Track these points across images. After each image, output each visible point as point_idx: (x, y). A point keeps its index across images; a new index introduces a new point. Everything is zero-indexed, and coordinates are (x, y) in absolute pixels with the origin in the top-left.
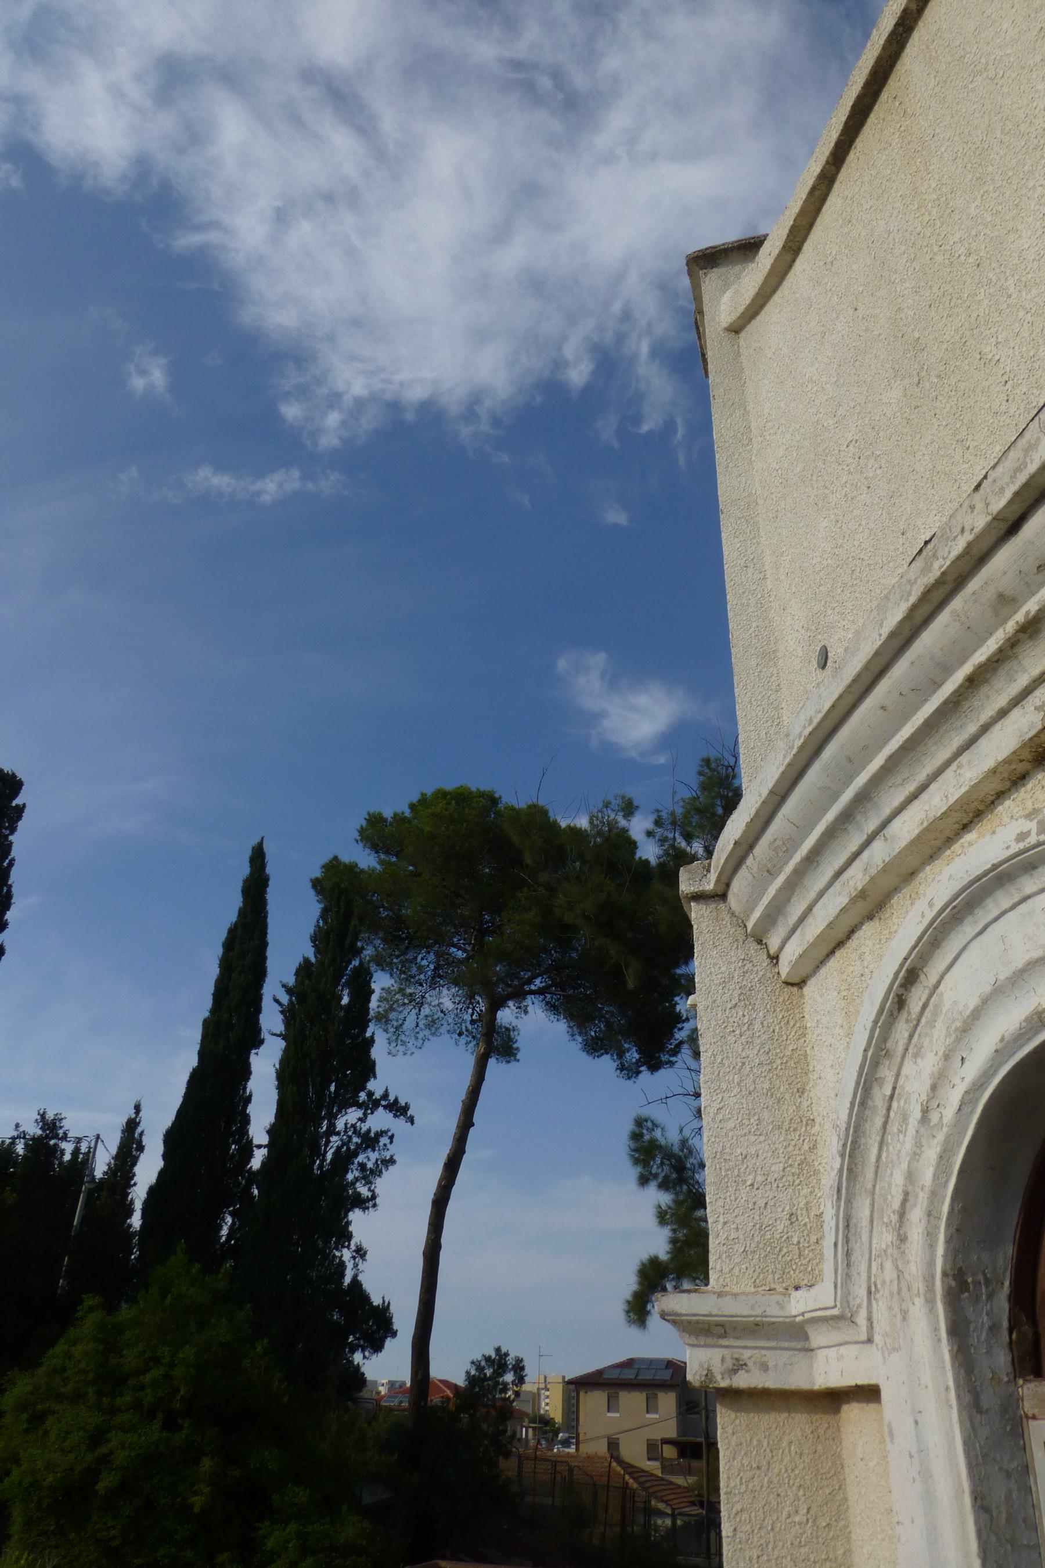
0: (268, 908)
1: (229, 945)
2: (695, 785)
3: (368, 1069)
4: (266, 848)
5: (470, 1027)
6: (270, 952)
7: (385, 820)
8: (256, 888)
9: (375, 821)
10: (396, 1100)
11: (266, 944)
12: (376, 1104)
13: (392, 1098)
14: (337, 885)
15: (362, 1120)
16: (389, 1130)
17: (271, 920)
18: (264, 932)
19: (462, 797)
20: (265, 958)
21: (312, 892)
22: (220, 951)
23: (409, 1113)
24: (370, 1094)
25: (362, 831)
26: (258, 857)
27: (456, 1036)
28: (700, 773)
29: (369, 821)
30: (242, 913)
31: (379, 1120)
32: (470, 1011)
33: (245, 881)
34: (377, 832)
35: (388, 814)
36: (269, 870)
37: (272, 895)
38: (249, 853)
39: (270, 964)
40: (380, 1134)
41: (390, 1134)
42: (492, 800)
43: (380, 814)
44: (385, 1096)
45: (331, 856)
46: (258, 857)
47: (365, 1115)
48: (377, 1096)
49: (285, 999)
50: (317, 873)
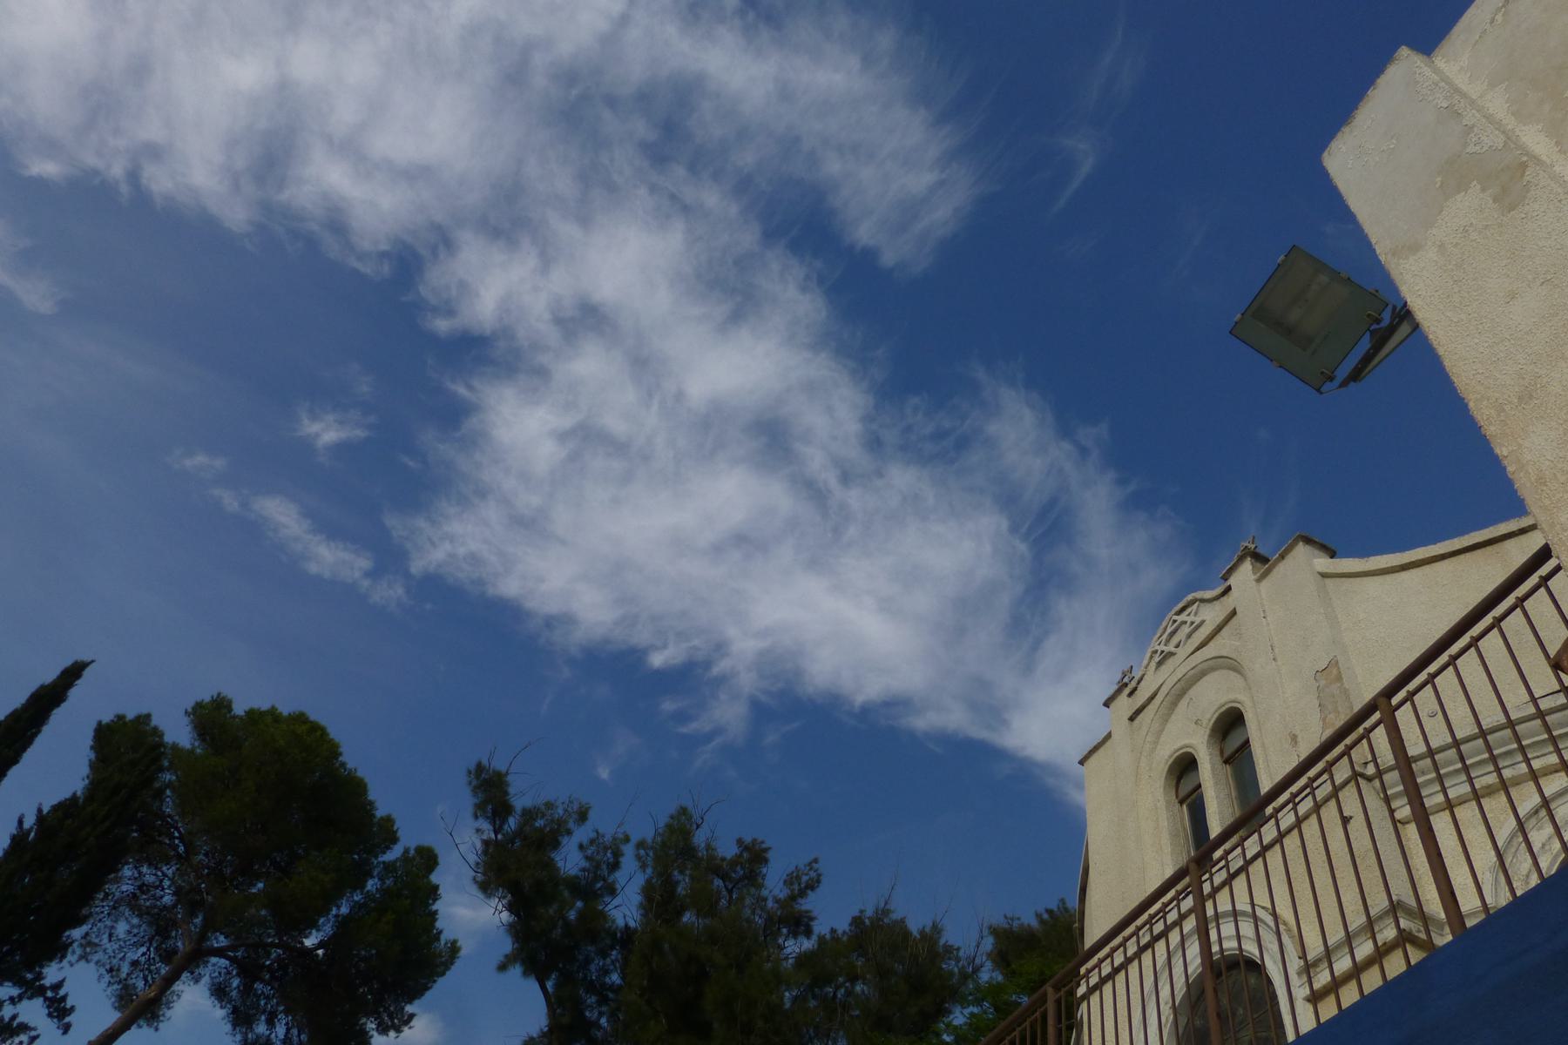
0: (45, 729)
2: (661, 825)
3: (57, 950)
5: (125, 969)
7: (230, 710)
9: (221, 705)
10: (64, 998)
11: (14, 760)
12: (40, 991)
13: (62, 992)
14: (125, 746)
15: (12, 1000)
16: (34, 1029)
17: (39, 741)
18: (24, 749)
19: (317, 730)
23: (67, 1020)
24: (39, 976)
25: (199, 706)
27: (103, 971)
28: (672, 817)
29: (213, 701)
30: (15, 716)
31: (33, 1012)
32: (144, 949)
33: (42, 687)
34: (211, 718)
35: (239, 709)
37: (58, 716)
40: (24, 1028)
41: (33, 1033)
42: (334, 751)
44: (57, 986)
45: (145, 712)
47: (20, 997)
48: (47, 982)
49: (29, 822)
50: (155, 722)
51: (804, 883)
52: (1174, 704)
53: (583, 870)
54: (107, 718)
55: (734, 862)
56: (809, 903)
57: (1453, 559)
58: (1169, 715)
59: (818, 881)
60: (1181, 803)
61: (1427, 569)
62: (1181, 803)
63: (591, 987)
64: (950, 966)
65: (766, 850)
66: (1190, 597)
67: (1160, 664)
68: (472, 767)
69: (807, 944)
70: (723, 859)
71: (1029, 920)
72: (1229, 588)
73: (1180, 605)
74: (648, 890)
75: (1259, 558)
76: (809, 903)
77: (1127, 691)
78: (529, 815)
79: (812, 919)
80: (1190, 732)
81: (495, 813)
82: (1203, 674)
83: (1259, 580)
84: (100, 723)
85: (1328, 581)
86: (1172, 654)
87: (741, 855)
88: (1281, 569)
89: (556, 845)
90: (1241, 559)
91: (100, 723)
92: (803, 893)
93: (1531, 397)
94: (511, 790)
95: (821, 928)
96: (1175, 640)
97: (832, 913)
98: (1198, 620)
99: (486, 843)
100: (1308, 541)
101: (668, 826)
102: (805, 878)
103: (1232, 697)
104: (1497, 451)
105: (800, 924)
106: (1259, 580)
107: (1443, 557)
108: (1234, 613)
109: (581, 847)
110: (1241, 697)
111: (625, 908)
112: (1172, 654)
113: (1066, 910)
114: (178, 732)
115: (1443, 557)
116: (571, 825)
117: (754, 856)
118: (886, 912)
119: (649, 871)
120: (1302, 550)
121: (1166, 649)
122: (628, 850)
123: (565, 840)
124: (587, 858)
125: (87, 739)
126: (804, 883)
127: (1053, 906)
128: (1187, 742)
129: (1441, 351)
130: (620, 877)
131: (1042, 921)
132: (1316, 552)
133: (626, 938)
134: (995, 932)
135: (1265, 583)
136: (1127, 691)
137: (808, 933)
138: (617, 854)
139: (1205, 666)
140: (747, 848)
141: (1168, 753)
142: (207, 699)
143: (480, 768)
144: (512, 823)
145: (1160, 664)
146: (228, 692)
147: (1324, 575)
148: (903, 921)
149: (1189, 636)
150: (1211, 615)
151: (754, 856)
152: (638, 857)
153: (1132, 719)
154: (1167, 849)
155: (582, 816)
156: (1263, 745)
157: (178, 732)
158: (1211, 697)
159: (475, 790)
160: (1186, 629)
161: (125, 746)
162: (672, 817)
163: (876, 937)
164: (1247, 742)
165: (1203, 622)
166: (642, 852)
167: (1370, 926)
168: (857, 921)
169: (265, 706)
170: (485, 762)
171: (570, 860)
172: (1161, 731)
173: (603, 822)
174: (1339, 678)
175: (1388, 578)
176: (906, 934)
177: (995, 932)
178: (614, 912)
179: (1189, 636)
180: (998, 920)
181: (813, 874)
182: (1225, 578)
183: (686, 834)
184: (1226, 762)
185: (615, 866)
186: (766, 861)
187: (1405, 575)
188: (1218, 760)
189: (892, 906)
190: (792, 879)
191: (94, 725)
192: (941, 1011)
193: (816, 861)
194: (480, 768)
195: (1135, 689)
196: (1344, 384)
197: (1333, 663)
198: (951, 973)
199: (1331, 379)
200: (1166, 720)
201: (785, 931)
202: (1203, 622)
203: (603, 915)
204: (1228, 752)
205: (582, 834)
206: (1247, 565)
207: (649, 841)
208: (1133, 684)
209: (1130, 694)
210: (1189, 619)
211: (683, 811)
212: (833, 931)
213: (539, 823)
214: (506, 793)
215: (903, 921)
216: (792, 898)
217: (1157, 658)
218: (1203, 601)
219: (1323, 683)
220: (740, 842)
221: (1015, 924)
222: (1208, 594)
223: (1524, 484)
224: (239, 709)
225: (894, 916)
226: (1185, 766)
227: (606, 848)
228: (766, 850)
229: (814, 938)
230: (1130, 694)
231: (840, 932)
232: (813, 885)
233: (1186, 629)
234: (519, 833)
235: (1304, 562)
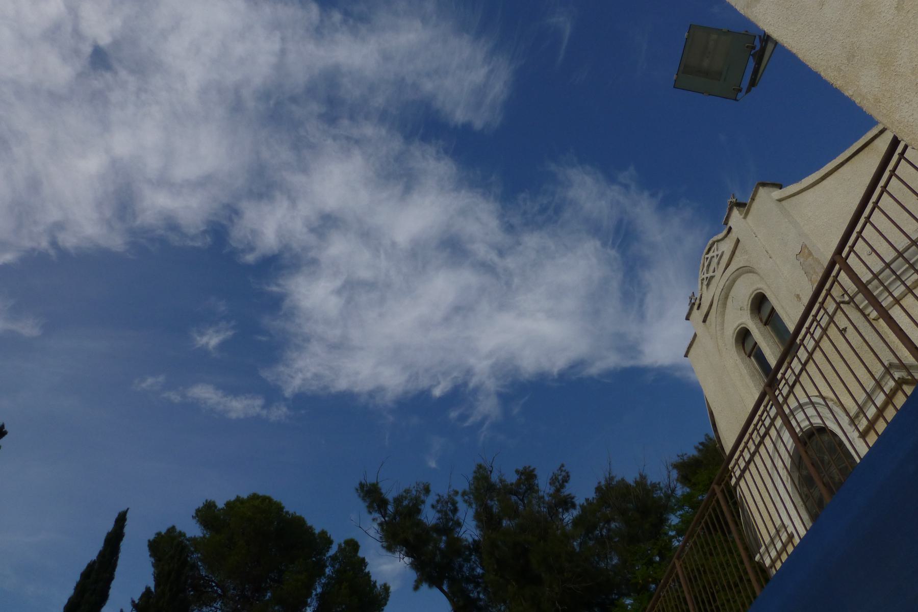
0: (120, 555)
1: (86, 575)
2: (471, 478)
4: (128, 516)
6: (114, 584)
7: (215, 506)
8: (114, 540)
9: (210, 506)
11: (111, 578)
14: (167, 548)
17: (119, 562)
19: (266, 500)
20: (109, 588)
21: (147, 548)
22: (78, 578)
26: (121, 520)
29: (205, 506)
30: (101, 555)
34: (207, 514)
35: (220, 504)
36: (127, 530)
37: (124, 545)
38: (116, 515)
39: (112, 592)
42: (279, 508)
43: (214, 502)
45: (170, 525)
46: (121, 520)
50: (178, 529)
51: (561, 480)
52: (725, 305)
53: (439, 519)
54: (152, 537)
55: (518, 484)
56: (568, 490)
57: (849, 163)
58: (724, 311)
59: (568, 476)
60: (749, 356)
61: (836, 174)
62: (749, 356)
63: (468, 580)
64: (659, 494)
65: (533, 470)
66: (710, 242)
67: (708, 285)
68: (358, 486)
69: (575, 513)
70: (512, 484)
71: (692, 452)
72: (730, 228)
73: (707, 248)
74: (477, 517)
75: (740, 205)
76: (568, 490)
77: (696, 307)
78: (398, 500)
79: (573, 498)
80: (739, 315)
81: (379, 507)
82: (734, 281)
83: (745, 218)
84: (149, 541)
85: (783, 203)
86: (712, 277)
87: (520, 478)
88: (755, 206)
89: (419, 511)
90: (731, 210)
91: (149, 541)
92: (562, 486)
93: (854, 56)
94: (383, 491)
95: (580, 500)
96: (711, 269)
97: (582, 491)
98: (720, 253)
99: (381, 524)
100: (764, 185)
101: (475, 478)
102: (560, 478)
103: (755, 287)
104: (846, 94)
105: (567, 503)
106: (745, 218)
107: (842, 164)
108: (738, 241)
109: (433, 507)
110: (759, 286)
111: (469, 530)
112: (712, 277)
113: (711, 439)
114: (193, 530)
115: (842, 164)
116: (422, 497)
117: (528, 476)
118: (611, 479)
119: (474, 506)
120: (762, 191)
121: (708, 275)
122: (459, 499)
123: (422, 507)
124: (438, 512)
125: (146, 552)
126: (561, 480)
127: (703, 440)
128: (740, 322)
129: (794, 51)
130: (460, 515)
131: (699, 450)
132: (771, 189)
133: (476, 547)
134: (675, 466)
135: (750, 217)
136: (696, 307)
137: (574, 506)
138: (454, 503)
139: (733, 276)
140: (522, 474)
141: (732, 332)
142: (201, 505)
143: (362, 486)
144: (391, 508)
145: (708, 285)
146: (211, 498)
147: (780, 200)
148: (623, 480)
149: (718, 263)
150: (726, 247)
151: (528, 476)
152: (466, 501)
153: (704, 321)
154: (751, 384)
155: (427, 490)
156: (783, 307)
157: (193, 530)
158: (744, 292)
159: (364, 500)
160: (715, 260)
161: (167, 548)
162: (475, 472)
163: (613, 495)
164: (773, 308)
165: (723, 253)
166: (466, 497)
167: (879, 385)
168: (598, 489)
169: (233, 498)
170: (363, 482)
171: (429, 516)
172: (723, 323)
173: (440, 489)
174: (810, 254)
175: (816, 187)
176: (628, 486)
177: (675, 466)
178: (464, 536)
179: (718, 263)
180: (675, 459)
181: (563, 474)
182: (726, 223)
183: (486, 479)
184: (765, 324)
185: (455, 510)
186: (535, 476)
187: (825, 182)
188: (761, 325)
189: (613, 474)
190: (553, 481)
191: (147, 543)
192: (662, 521)
193: (563, 466)
194: (362, 486)
195: (700, 304)
196: (748, 90)
197: (804, 247)
198: (660, 498)
199: (740, 90)
200: (723, 314)
201: (560, 510)
202: (723, 253)
203: (459, 540)
204: (764, 320)
205: (431, 500)
206: (735, 212)
207: (467, 489)
208: (698, 301)
209: (698, 308)
210: (715, 254)
211: (480, 467)
212: (587, 500)
213: (405, 503)
214: (381, 494)
215: (623, 480)
216: (558, 491)
217: (705, 283)
218: (718, 241)
219: (802, 260)
220: (517, 472)
221: (685, 458)
222: (720, 236)
223: (868, 106)
224: (220, 504)
225: (618, 478)
226: (743, 335)
227: (447, 503)
228: (533, 470)
229: (578, 507)
230: (698, 308)
231: (591, 498)
232: (566, 479)
233: (715, 260)
234: (396, 512)
235: (767, 197)
